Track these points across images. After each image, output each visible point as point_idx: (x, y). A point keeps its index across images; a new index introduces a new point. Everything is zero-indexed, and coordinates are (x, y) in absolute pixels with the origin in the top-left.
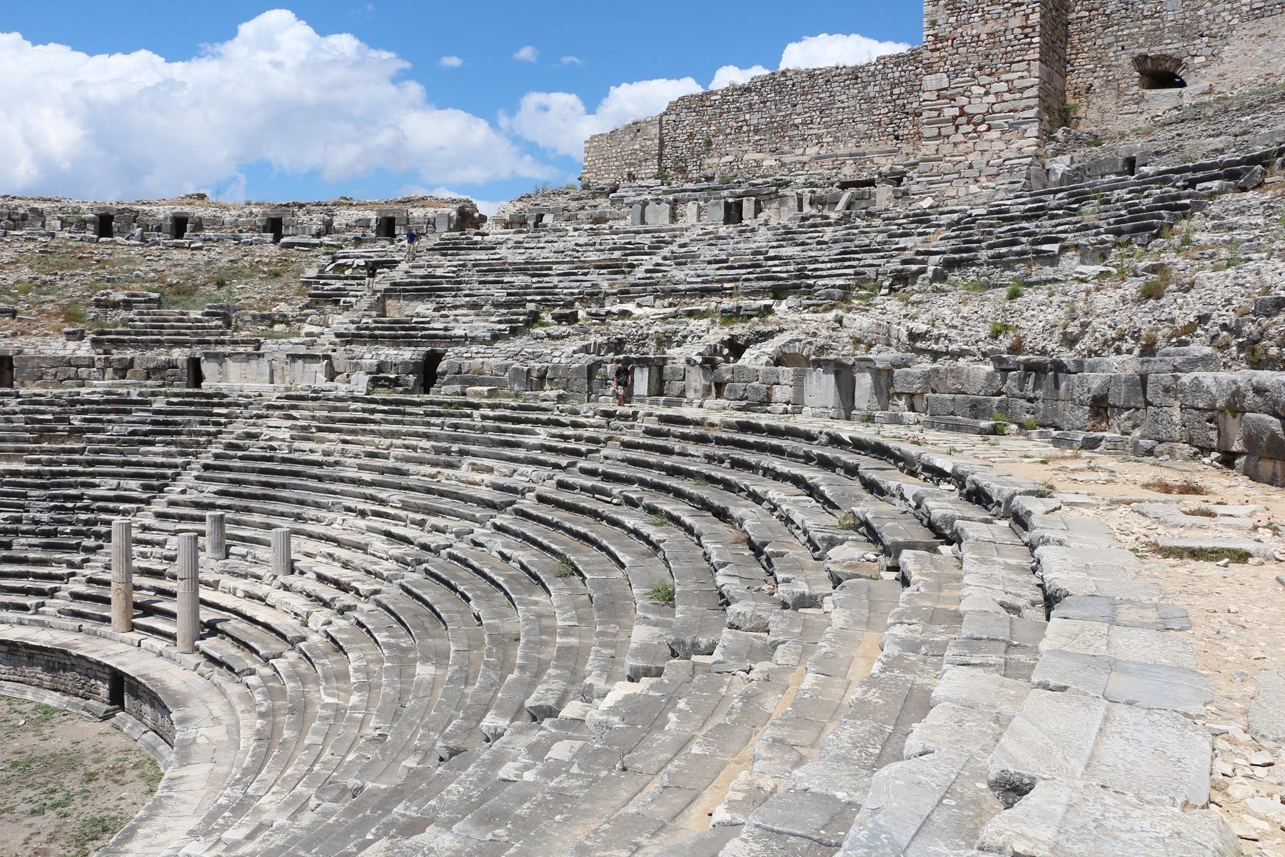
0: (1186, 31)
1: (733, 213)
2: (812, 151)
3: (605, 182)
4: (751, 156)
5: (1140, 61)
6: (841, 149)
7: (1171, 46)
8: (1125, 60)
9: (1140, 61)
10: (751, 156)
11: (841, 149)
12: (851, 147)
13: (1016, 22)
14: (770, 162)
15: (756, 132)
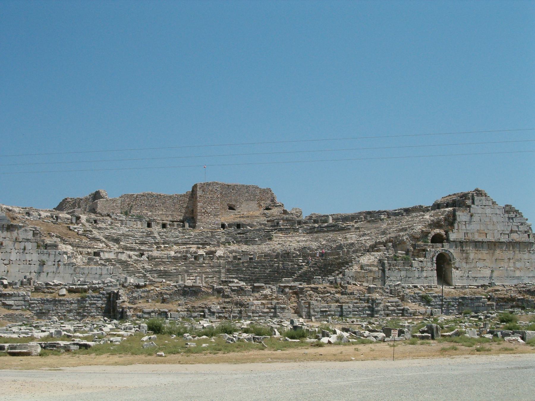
0: (236, 201)
1: (149, 225)
2: (161, 212)
3: (105, 212)
4: (145, 212)
5: (228, 204)
6: (168, 213)
7: (234, 203)
8: (226, 204)
9: (228, 204)
10: (145, 212)
11: (168, 213)
12: (170, 213)
13: (215, 196)
14: (150, 213)
15: (146, 206)
